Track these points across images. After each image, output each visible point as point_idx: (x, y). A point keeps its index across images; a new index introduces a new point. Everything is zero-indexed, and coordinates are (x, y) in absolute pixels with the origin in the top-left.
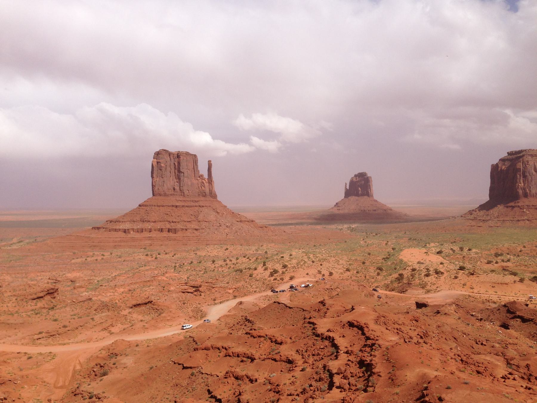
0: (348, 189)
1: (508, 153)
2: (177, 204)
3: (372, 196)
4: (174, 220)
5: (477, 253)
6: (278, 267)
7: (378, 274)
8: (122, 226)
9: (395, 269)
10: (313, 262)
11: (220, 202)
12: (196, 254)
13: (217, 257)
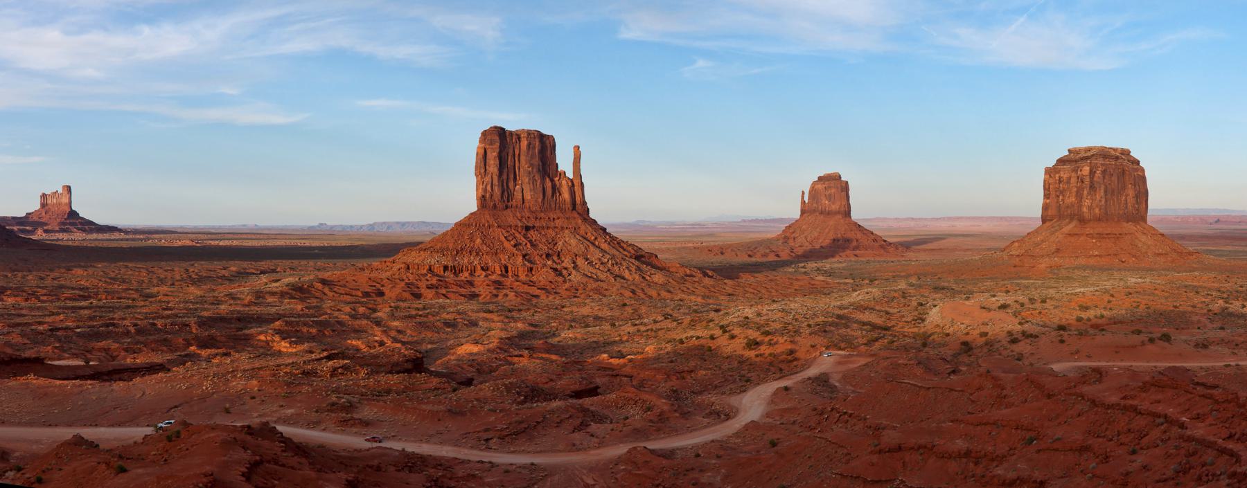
0: (807, 202)
3: (847, 213)
11: (595, 221)
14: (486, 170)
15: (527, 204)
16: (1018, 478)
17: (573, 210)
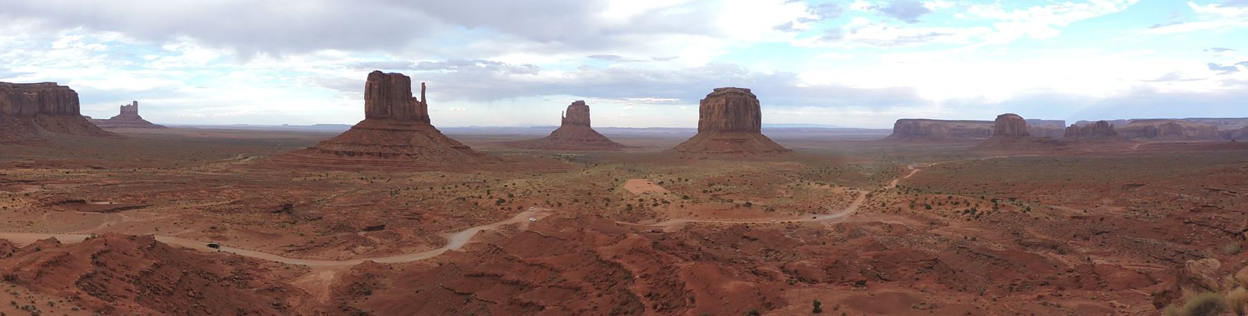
1: (715, 90)
2: (389, 128)
3: (588, 124)
4: (387, 145)
5: (693, 184)
6: (504, 196)
7: (607, 205)
8: (335, 148)
9: (623, 199)
10: (539, 192)
12: (411, 180)
13: (434, 184)
16: (531, 302)
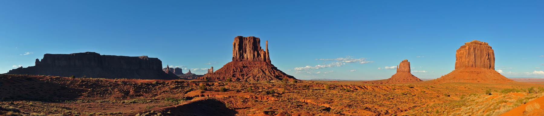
14: (235, 49)
15: (248, 60)
17: (264, 61)
